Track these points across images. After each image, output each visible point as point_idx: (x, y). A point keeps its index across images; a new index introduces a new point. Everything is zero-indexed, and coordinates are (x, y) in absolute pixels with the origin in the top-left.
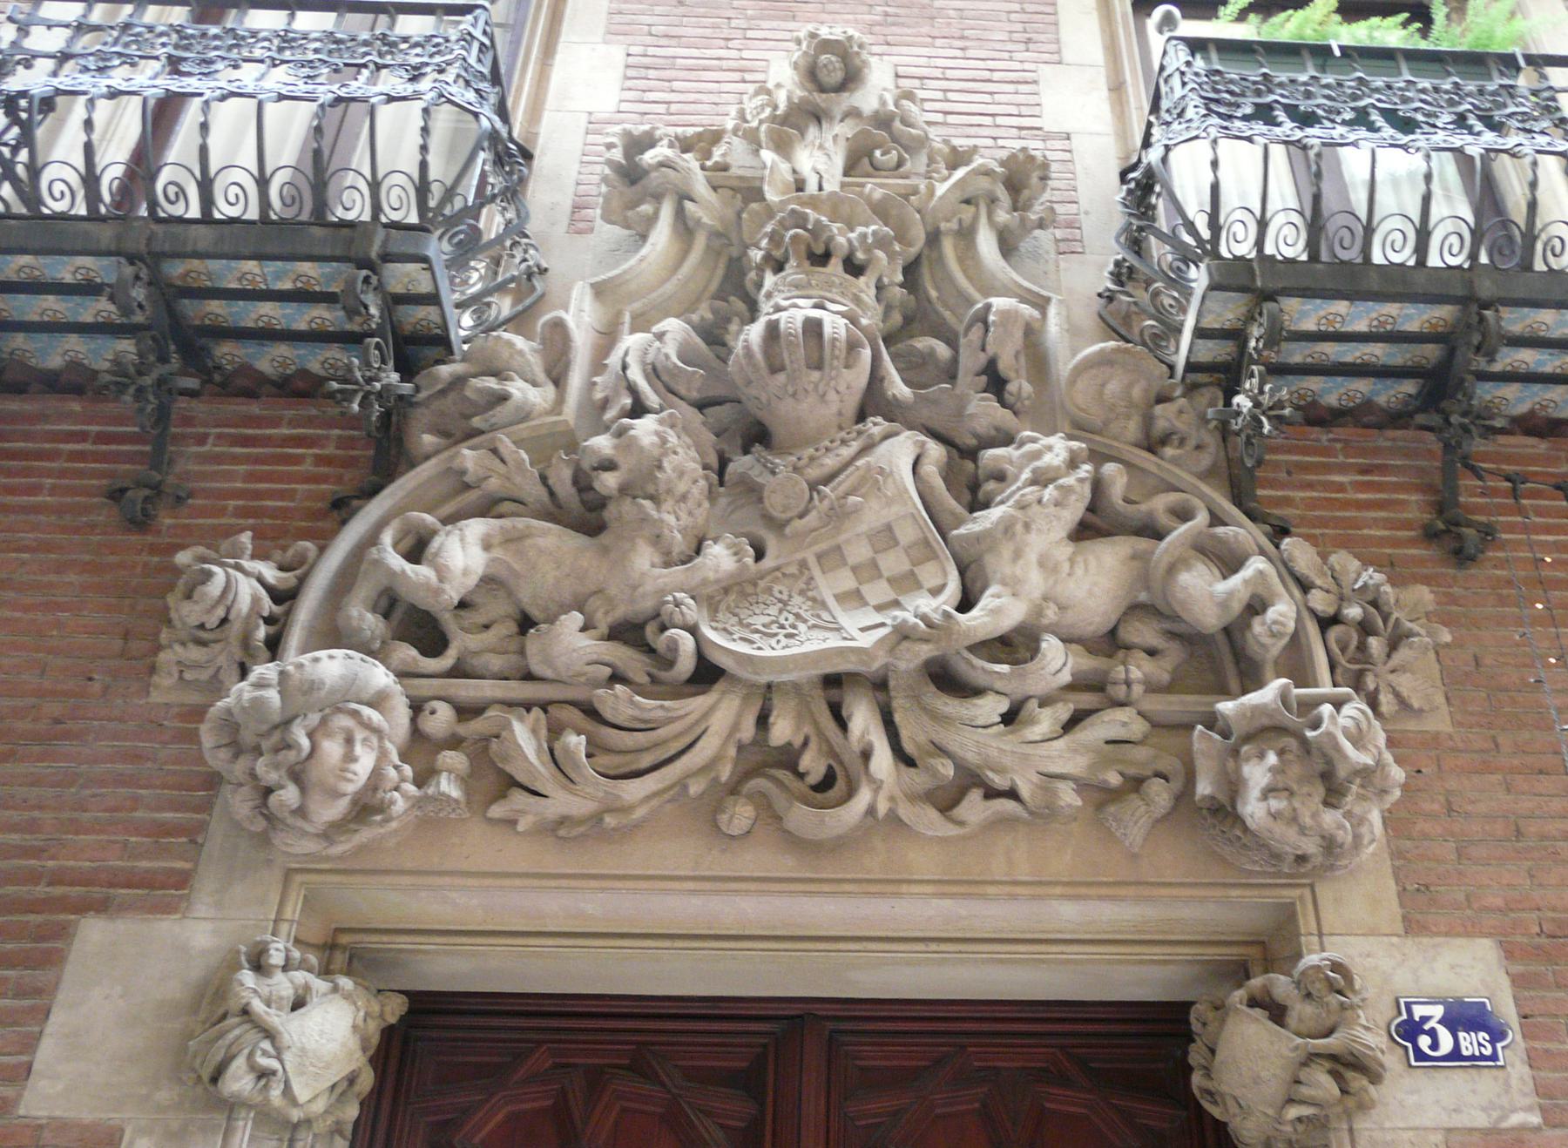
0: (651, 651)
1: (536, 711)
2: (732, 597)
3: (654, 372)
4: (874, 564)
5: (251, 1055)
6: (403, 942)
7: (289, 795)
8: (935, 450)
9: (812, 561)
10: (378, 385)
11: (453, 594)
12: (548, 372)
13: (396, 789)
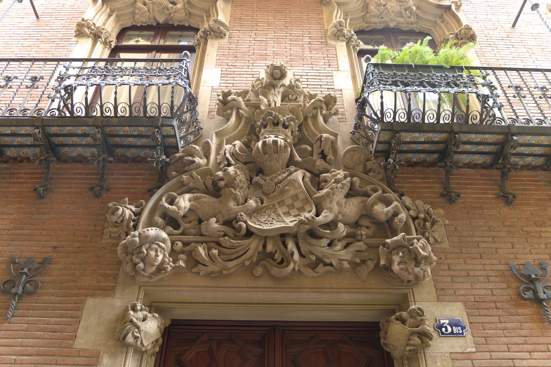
0: (234, 228)
1: (204, 244)
2: (255, 214)
3: (232, 155)
4: (293, 205)
5: (133, 333)
6: (170, 305)
8: (308, 174)
10: (161, 159)
11: (182, 213)
12: (205, 156)
13: (168, 264)
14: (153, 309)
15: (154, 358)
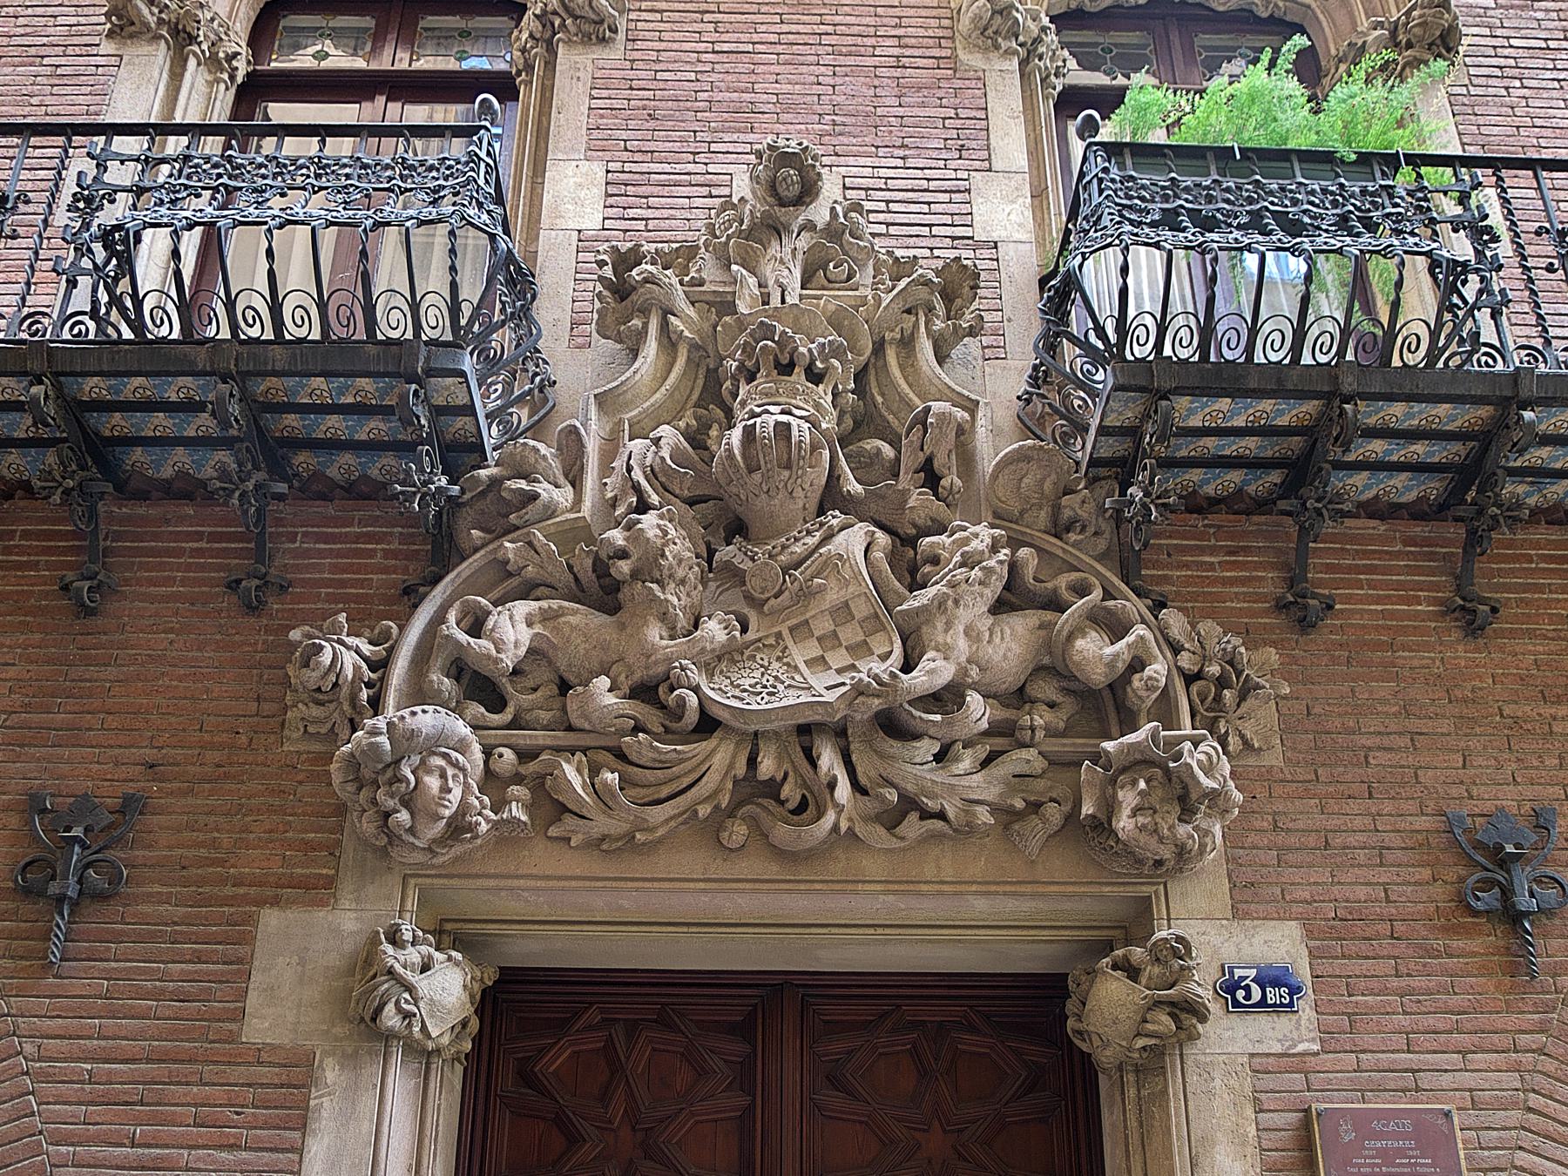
0: (663, 707)
2: (723, 666)
3: (652, 474)
5: (397, 1003)
8: (882, 538)
9: (786, 633)
11: (508, 661)
12: (566, 476)
13: (480, 814)
14: (446, 940)
15: (459, 1069)
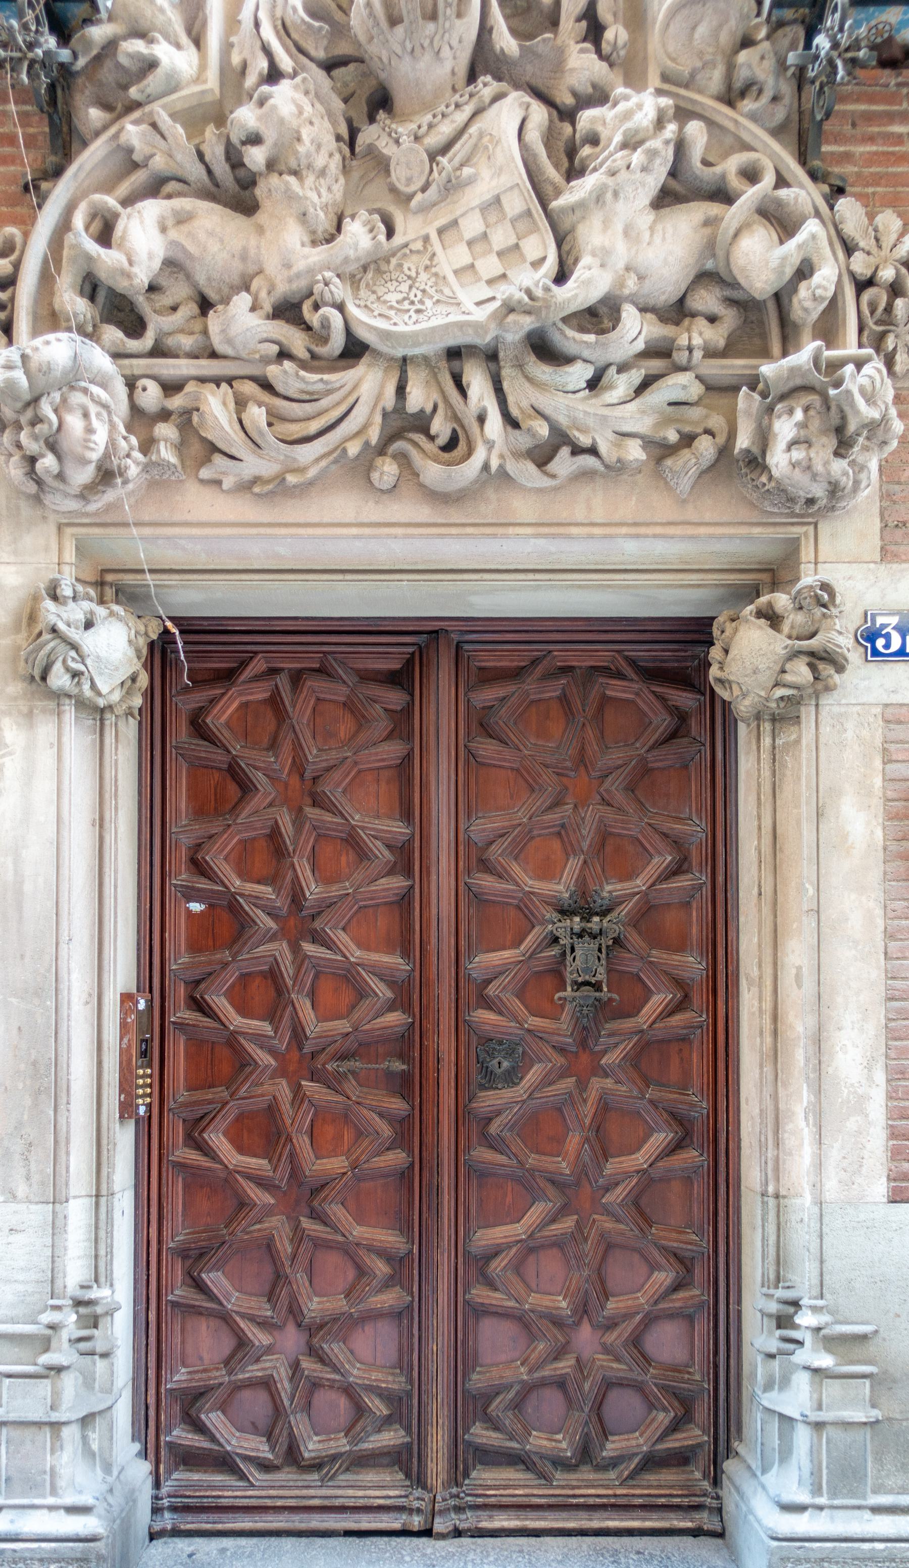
0: (309, 328)
1: (224, 385)
2: (370, 275)
3: (284, 29)
7: (48, 462)
8: (539, 114)
9: (434, 236)
10: (39, 52)
11: (142, 276)
12: (189, 32)
13: (128, 456)
14: (109, 592)
15: (133, 723)
